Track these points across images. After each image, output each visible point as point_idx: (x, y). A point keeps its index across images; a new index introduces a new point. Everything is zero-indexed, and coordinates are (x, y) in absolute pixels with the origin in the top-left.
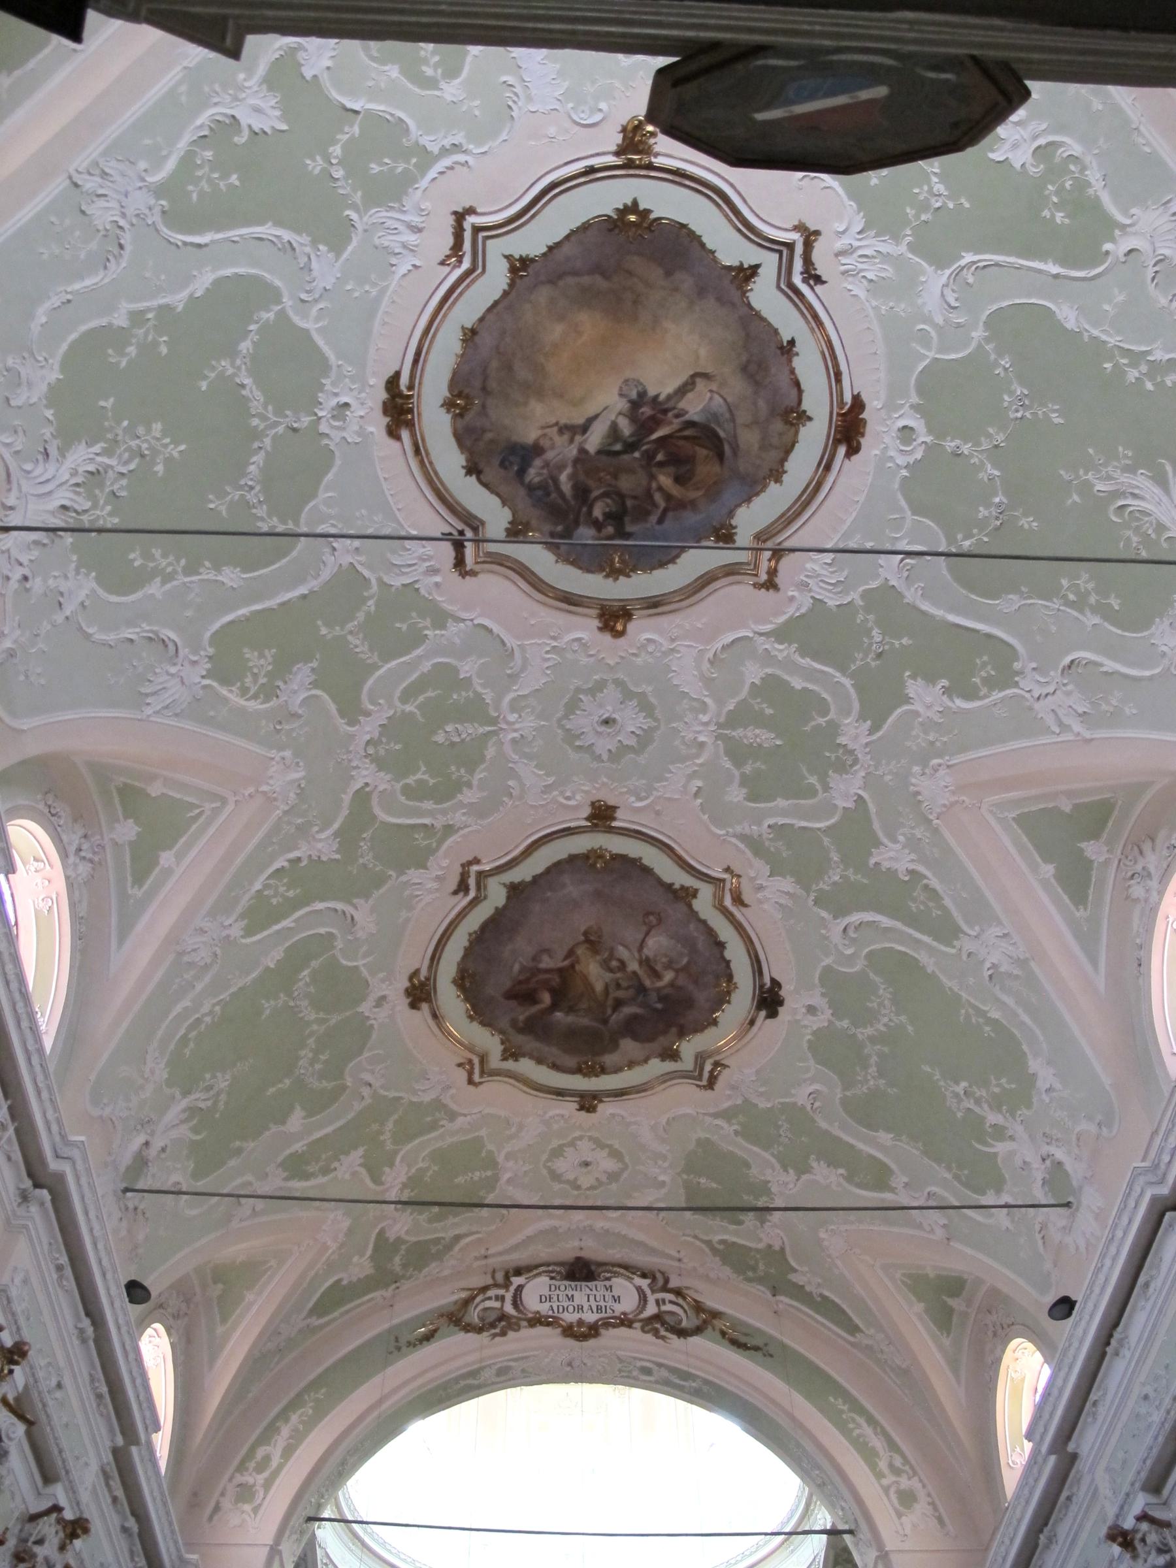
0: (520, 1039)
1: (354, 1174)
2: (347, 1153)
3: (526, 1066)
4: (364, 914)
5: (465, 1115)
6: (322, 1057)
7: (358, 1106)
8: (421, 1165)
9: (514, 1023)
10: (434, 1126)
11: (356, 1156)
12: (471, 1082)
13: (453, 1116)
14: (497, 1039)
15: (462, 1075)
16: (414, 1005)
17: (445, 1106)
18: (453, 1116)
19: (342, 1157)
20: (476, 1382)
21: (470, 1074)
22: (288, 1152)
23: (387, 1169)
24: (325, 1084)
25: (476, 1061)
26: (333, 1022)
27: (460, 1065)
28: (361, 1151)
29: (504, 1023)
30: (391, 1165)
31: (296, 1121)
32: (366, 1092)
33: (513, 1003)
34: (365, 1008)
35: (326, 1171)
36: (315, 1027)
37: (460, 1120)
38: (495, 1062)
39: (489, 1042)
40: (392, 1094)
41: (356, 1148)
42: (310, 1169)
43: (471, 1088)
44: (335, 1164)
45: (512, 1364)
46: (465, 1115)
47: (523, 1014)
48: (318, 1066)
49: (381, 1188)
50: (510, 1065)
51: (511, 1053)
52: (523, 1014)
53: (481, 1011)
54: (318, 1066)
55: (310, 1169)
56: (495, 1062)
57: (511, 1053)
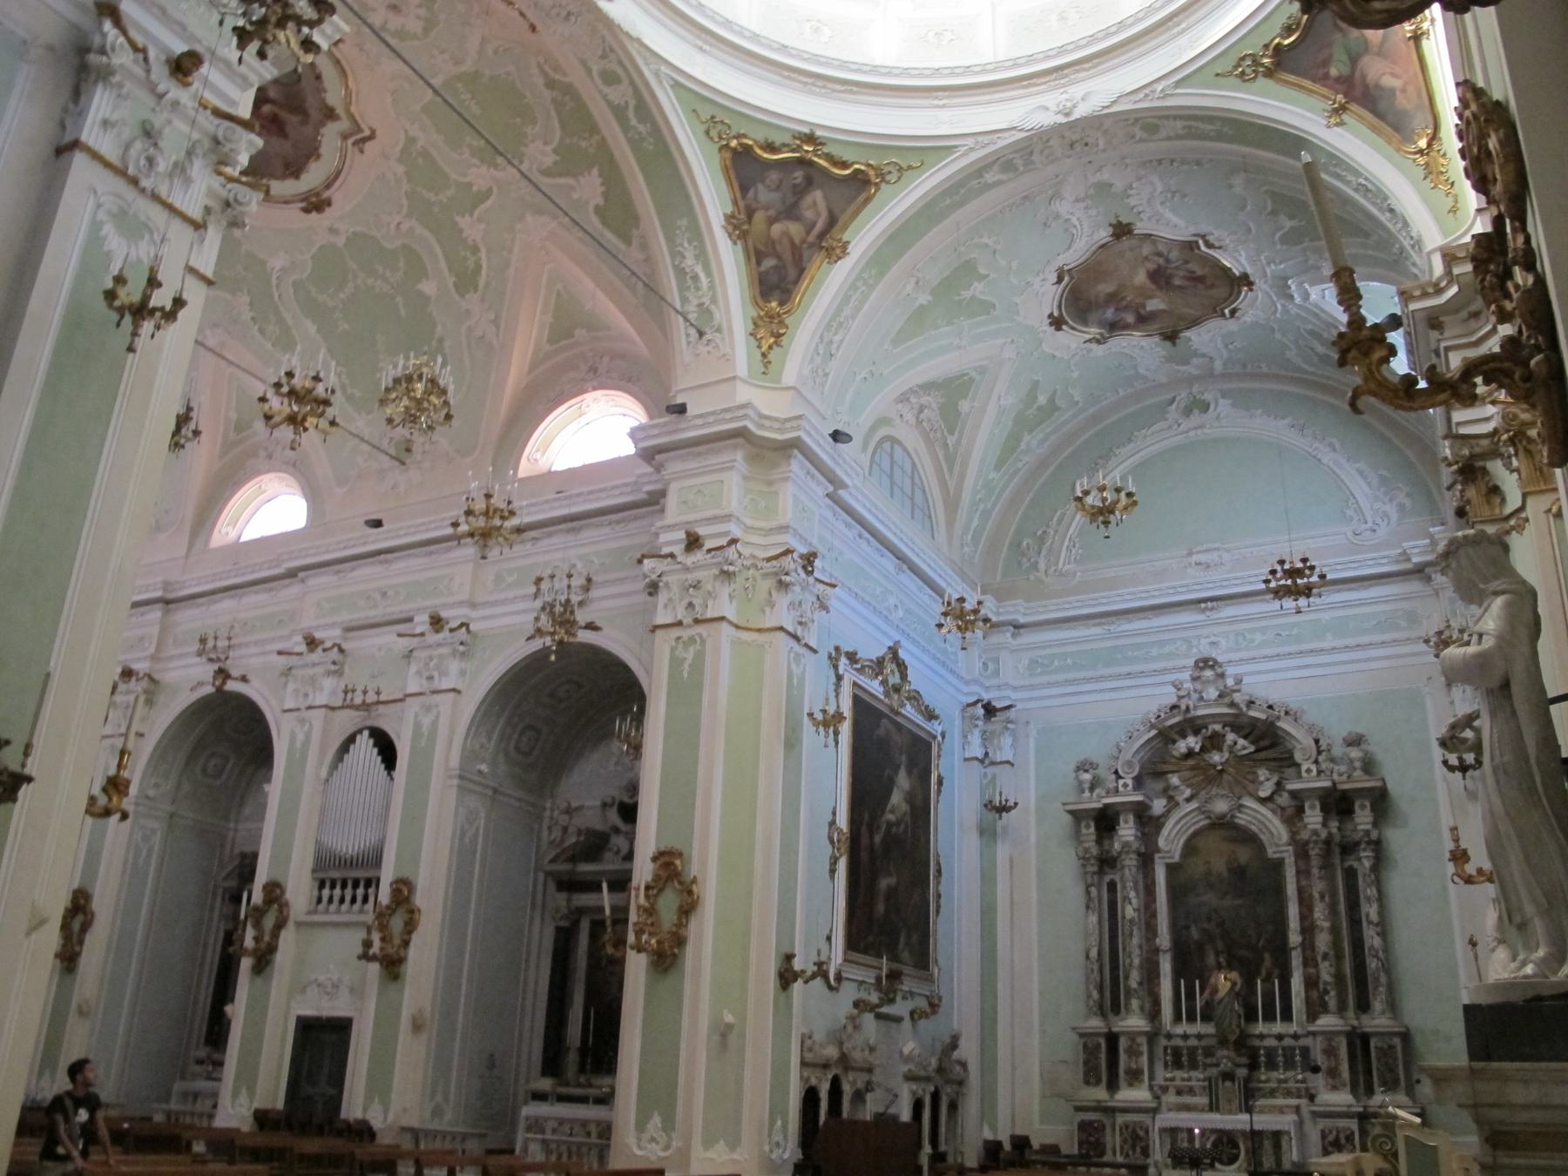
0: (315, 114)
1: (479, 220)
2: (461, 231)
3: (334, 97)
4: (277, 263)
5: (406, 131)
6: (381, 271)
7: (420, 230)
8: (466, 155)
9: (305, 122)
10: (426, 154)
11: (464, 222)
12: (372, 137)
13: (411, 140)
14: (324, 130)
15: (368, 146)
16: (329, 203)
17: (402, 151)
18: (411, 140)
19: (464, 235)
20: (632, 103)
21: (364, 140)
22: (453, 290)
23: (475, 188)
24: (401, 264)
25: (350, 141)
26: (355, 266)
27: (362, 151)
28: (458, 219)
29: (308, 130)
30: (469, 185)
31: (428, 287)
32: (405, 227)
33: (288, 129)
34: (340, 241)
35: (475, 249)
36: (359, 281)
37: (412, 133)
38: (343, 125)
39: (330, 136)
40: (405, 202)
41: (456, 224)
42: (471, 263)
43: (378, 133)
44: (470, 241)
45: (595, 73)
46: (406, 131)
47: (292, 120)
48: (388, 274)
49: (495, 191)
50: (340, 110)
51: (330, 114)
52: (292, 120)
53: (311, 152)
54: (388, 274)
55: (471, 263)
56: (343, 125)
57: (330, 114)
